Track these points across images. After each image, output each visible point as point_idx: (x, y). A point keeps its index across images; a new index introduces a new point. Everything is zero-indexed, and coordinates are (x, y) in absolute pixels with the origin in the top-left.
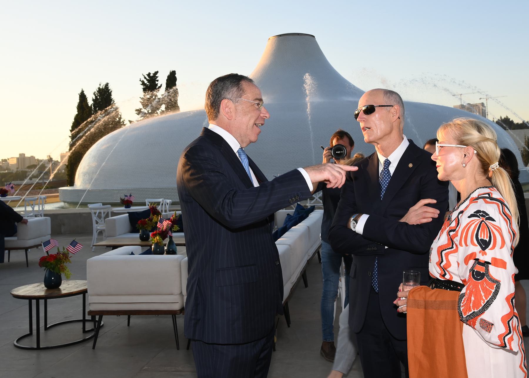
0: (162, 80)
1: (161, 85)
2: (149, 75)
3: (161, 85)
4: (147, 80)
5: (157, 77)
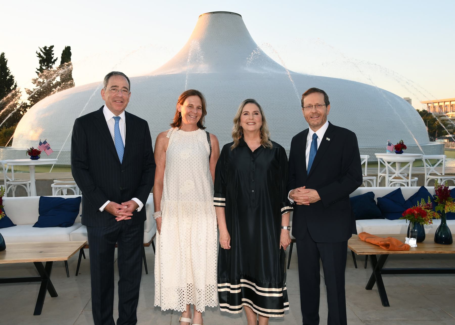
0: (57, 54)
1: (57, 59)
2: (45, 48)
3: (57, 59)
4: (43, 53)
5: (53, 51)
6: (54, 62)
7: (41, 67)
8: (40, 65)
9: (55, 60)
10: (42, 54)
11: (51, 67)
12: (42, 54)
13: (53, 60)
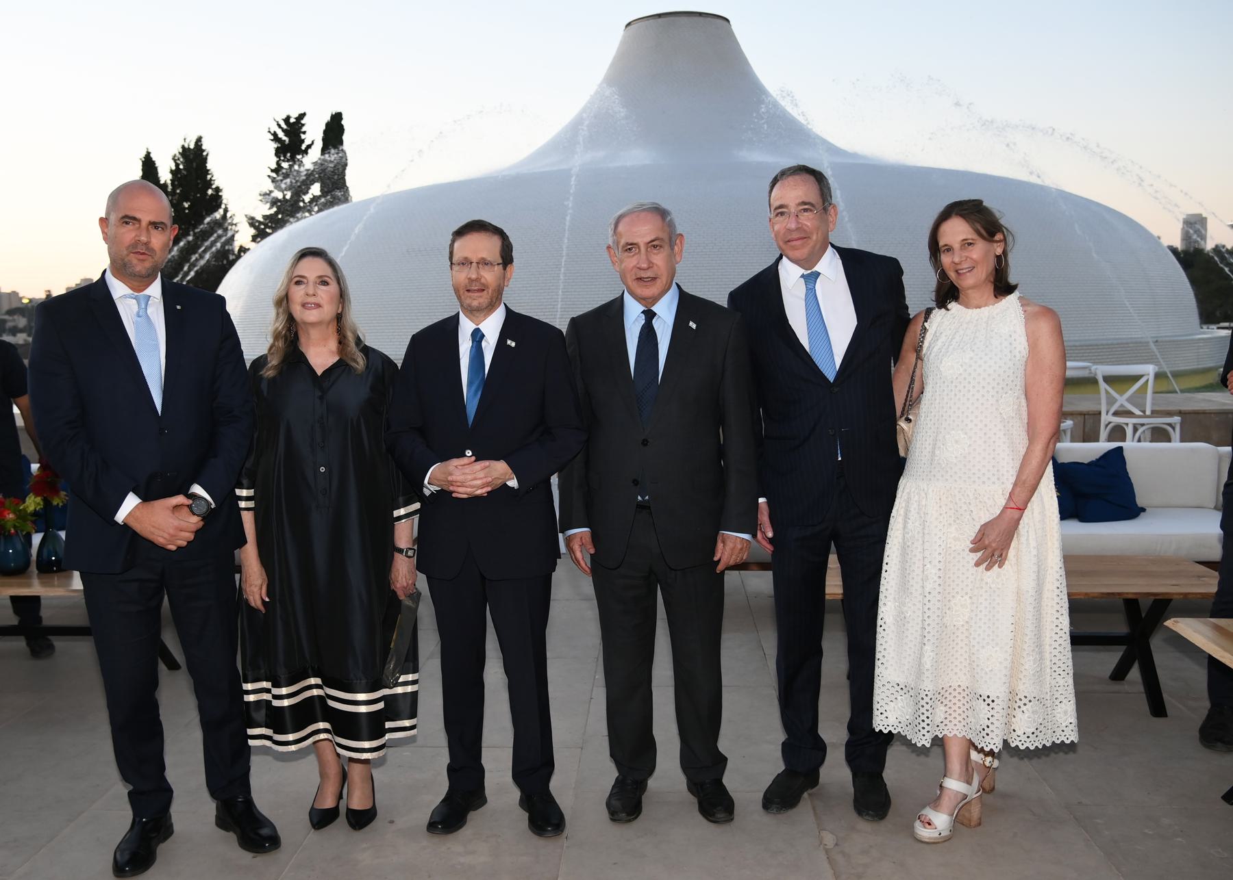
6: (306, 152)
7: (278, 163)
8: (276, 159)
9: (309, 147)
10: (281, 135)
11: (301, 164)
12: (281, 135)
13: (303, 147)
